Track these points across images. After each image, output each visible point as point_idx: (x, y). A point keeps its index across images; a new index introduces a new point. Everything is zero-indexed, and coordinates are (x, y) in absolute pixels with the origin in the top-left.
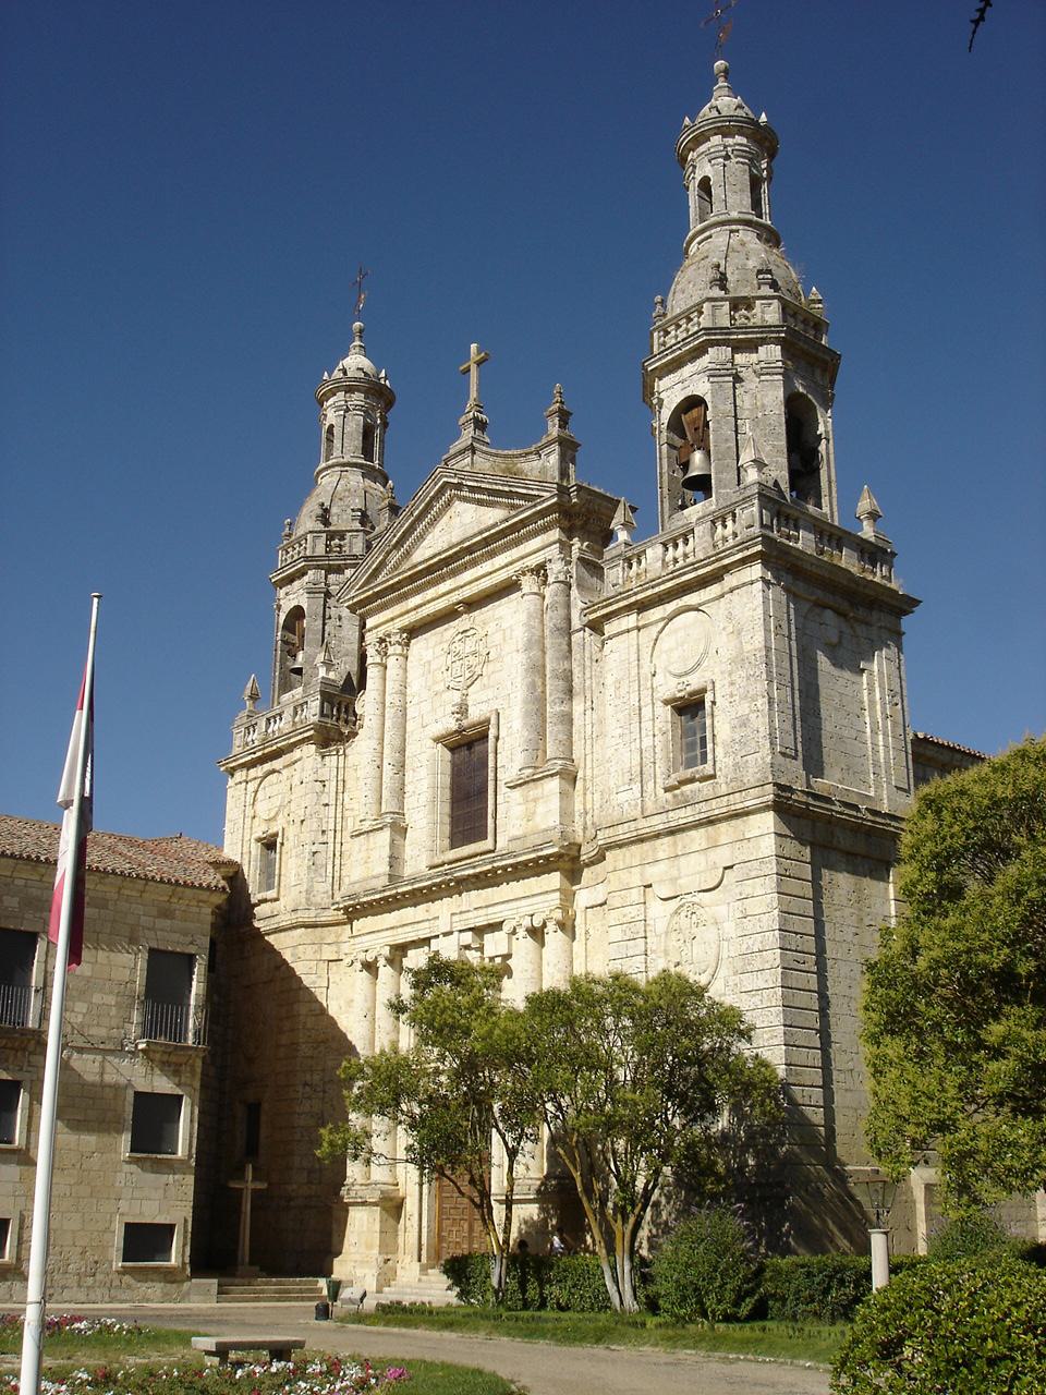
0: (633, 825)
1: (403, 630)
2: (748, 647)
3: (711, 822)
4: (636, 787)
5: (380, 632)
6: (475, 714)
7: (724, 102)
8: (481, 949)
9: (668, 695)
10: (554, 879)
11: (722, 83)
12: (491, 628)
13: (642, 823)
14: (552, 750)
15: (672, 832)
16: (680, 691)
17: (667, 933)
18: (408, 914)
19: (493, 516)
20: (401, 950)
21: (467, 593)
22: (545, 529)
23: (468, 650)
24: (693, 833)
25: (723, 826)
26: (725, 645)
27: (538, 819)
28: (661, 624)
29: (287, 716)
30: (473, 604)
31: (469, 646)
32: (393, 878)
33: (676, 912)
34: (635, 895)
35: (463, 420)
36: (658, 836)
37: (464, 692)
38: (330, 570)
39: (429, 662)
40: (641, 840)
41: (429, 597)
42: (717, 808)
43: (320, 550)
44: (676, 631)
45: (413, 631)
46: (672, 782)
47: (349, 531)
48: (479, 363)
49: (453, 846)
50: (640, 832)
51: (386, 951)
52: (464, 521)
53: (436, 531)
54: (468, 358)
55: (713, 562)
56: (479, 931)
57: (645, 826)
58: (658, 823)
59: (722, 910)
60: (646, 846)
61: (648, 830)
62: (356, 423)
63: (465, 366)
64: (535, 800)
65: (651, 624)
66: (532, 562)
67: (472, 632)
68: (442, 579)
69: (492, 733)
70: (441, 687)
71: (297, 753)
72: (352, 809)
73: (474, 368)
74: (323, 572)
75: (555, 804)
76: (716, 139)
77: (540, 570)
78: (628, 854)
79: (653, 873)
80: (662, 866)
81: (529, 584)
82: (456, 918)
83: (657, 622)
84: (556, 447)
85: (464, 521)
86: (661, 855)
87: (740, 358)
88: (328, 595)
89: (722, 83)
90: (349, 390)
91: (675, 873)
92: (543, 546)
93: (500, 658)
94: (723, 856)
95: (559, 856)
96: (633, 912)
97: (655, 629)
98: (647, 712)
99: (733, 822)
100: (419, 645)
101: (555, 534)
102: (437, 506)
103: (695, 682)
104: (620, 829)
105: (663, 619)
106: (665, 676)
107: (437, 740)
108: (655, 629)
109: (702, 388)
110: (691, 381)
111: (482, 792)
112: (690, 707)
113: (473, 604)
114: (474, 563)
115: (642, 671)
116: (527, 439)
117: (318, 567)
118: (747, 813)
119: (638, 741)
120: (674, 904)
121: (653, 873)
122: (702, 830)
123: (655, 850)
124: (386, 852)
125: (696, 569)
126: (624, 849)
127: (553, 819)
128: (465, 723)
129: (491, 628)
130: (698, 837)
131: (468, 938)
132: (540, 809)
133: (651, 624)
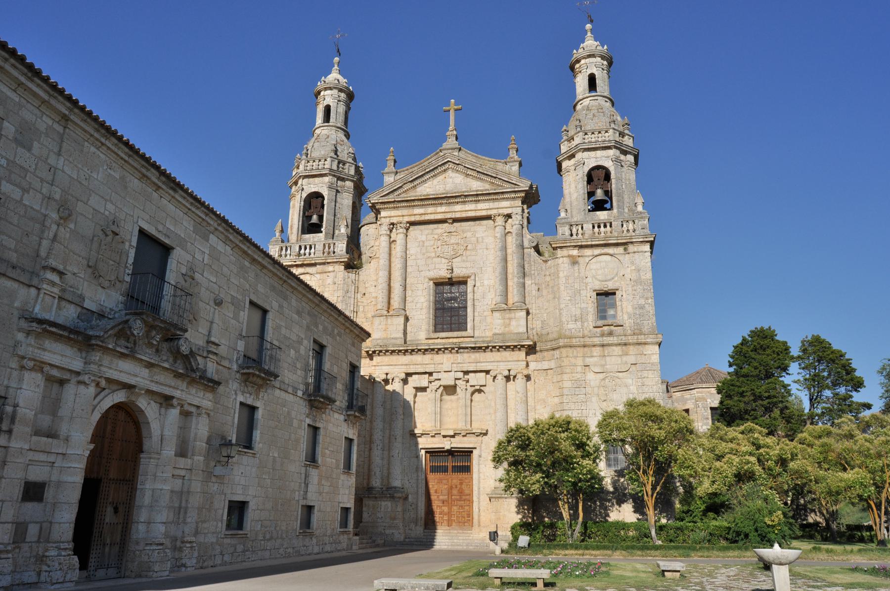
0: (582, 340)
1: (408, 222)
2: (643, 277)
3: (625, 344)
4: (579, 324)
5: (394, 220)
6: (459, 272)
7: (590, 43)
8: (468, 381)
9: (597, 288)
10: (522, 354)
11: (589, 34)
12: (469, 234)
14: (514, 296)
15: (603, 346)
17: (599, 387)
18: (418, 358)
19: (476, 186)
20: (409, 375)
21: (458, 215)
22: (514, 198)
23: (452, 241)
24: (614, 348)
25: (631, 348)
26: (629, 272)
27: (512, 328)
29: (319, 247)
30: (456, 220)
32: (405, 342)
33: (604, 379)
34: (579, 369)
35: (448, 133)
36: (594, 346)
38: (339, 179)
39: (423, 242)
40: (584, 346)
42: (631, 339)
43: (335, 167)
44: (600, 262)
45: (413, 224)
46: (600, 323)
48: (456, 110)
49: (436, 331)
51: (403, 376)
52: (451, 181)
53: (436, 181)
54: (449, 105)
56: (466, 373)
57: (588, 341)
58: (597, 341)
59: (630, 381)
60: (586, 349)
62: (342, 108)
63: (447, 108)
64: (510, 319)
66: (506, 211)
68: (442, 204)
69: (470, 283)
70: (433, 255)
71: (330, 268)
73: (452, 113)
75: (523, 322)
76: (599, 59)
77: (509, 216)
79: (588, 361)
80: (595, 359)
81: (500, 221)
83: (589, 256)
84: (517, 164)
85: (451, 181)
86: (595, 354)
87: (622, 157)
88: (338, 191)
89: (589, 34)
90: (341, 90)
91: (603, 363)
92: (514, 206)
93: (474, 249)
94: (631, 359)
95: (529, 346)
96: (579, 376)
97: (587, 259)
98: (583, 293)
99: (637, 346)
100: (415, 231)
101: (519, 203)
102: (440, 170)
103: (610, 286)
107: (431, 279)
108: (587, 259)
109: (609, 164)
110: (605, 159)
111: (436, 309)
112: (606, 295)
113: (456, 220)
114: (464, 202)
116: (501, 155)
117: (334, 176)
118: (645, 344)
120: (601, 376)
121: (588, 361)
122: (619, 347)
123: (591, 352)
127: (523, 329)
128: (454, 275)
129: (469, 234)
130: (617, 350)
131: (460, 375)
132: (513, 323)
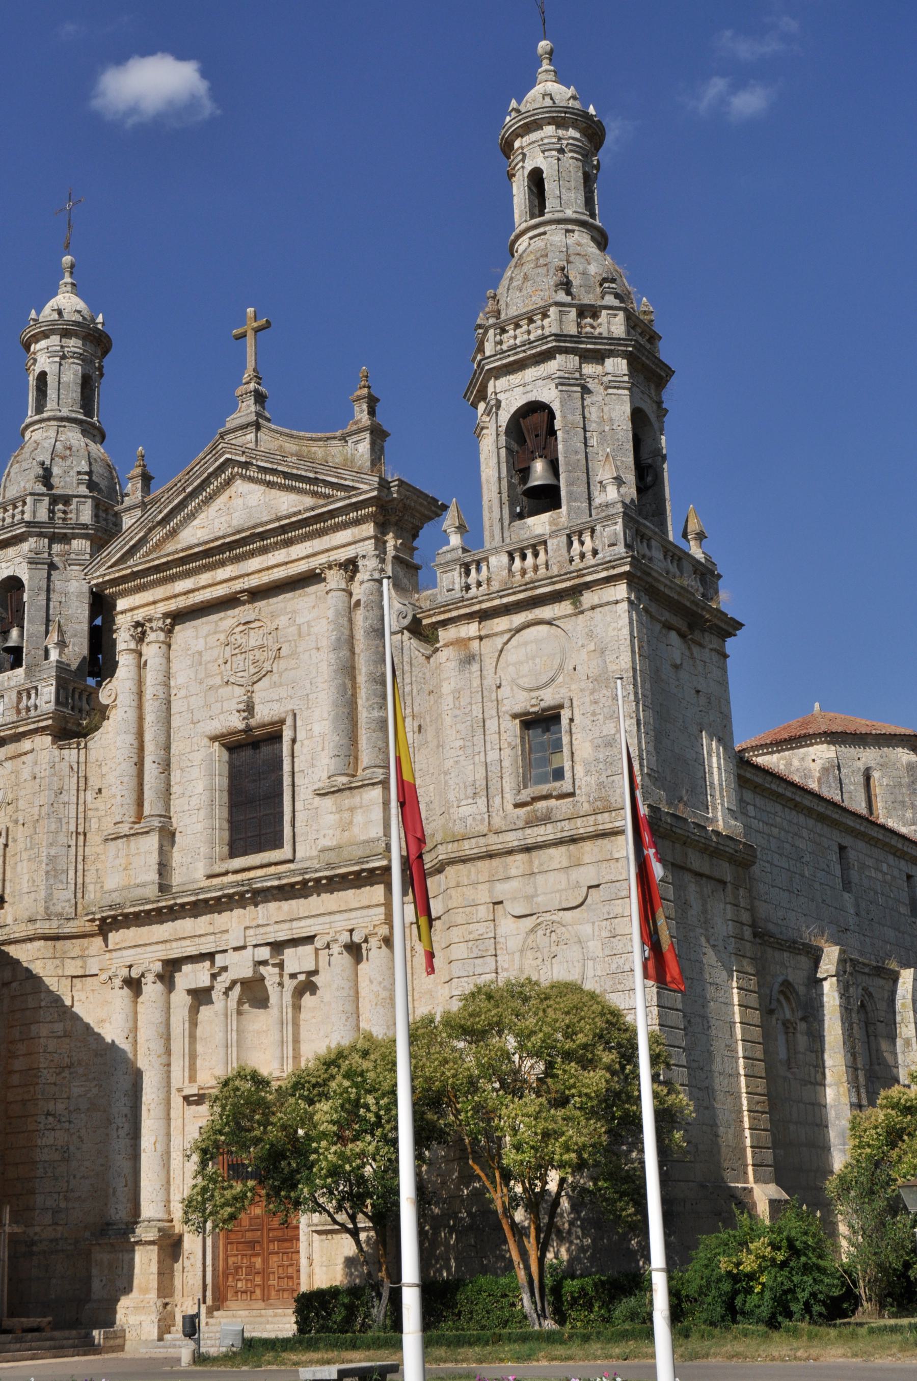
9: (518, 709)
13: (493, 839)
16: (533, 706)
28: (507, 636)
31: (254, 639)
37: (249, 688)
41: (202, 583)
44: (526, 644)
47: (77, 496)
50: (490, 848)
55: (574, 578)
61: (500, 846)
65: (495, 634)
67: (257, 624)
72: (97, 810)
74: (46, 540)
78: (473, 869)
82: (251, 932)
104: (466, 845)
105: (510, 630)
106: (512, 689)
115: (485, 682)
119: (482, 754)
123: (506, 867)
124: (154, 858)
125: (554, 583)
126: (468, 865)
133: (495, 634)
